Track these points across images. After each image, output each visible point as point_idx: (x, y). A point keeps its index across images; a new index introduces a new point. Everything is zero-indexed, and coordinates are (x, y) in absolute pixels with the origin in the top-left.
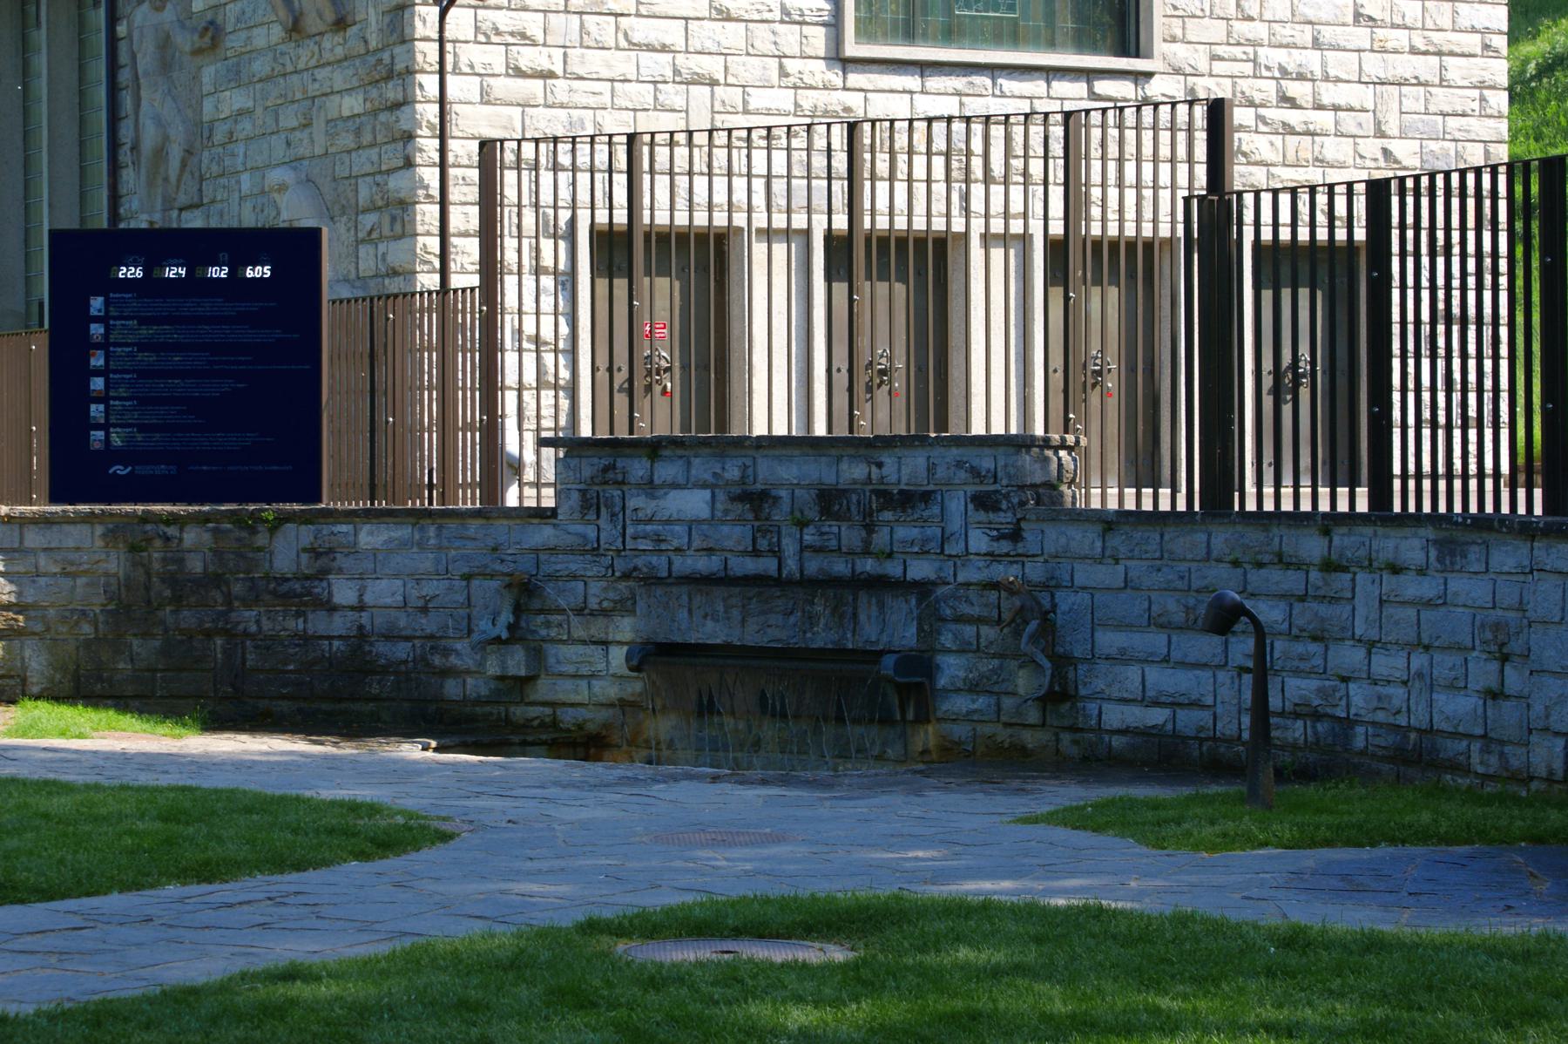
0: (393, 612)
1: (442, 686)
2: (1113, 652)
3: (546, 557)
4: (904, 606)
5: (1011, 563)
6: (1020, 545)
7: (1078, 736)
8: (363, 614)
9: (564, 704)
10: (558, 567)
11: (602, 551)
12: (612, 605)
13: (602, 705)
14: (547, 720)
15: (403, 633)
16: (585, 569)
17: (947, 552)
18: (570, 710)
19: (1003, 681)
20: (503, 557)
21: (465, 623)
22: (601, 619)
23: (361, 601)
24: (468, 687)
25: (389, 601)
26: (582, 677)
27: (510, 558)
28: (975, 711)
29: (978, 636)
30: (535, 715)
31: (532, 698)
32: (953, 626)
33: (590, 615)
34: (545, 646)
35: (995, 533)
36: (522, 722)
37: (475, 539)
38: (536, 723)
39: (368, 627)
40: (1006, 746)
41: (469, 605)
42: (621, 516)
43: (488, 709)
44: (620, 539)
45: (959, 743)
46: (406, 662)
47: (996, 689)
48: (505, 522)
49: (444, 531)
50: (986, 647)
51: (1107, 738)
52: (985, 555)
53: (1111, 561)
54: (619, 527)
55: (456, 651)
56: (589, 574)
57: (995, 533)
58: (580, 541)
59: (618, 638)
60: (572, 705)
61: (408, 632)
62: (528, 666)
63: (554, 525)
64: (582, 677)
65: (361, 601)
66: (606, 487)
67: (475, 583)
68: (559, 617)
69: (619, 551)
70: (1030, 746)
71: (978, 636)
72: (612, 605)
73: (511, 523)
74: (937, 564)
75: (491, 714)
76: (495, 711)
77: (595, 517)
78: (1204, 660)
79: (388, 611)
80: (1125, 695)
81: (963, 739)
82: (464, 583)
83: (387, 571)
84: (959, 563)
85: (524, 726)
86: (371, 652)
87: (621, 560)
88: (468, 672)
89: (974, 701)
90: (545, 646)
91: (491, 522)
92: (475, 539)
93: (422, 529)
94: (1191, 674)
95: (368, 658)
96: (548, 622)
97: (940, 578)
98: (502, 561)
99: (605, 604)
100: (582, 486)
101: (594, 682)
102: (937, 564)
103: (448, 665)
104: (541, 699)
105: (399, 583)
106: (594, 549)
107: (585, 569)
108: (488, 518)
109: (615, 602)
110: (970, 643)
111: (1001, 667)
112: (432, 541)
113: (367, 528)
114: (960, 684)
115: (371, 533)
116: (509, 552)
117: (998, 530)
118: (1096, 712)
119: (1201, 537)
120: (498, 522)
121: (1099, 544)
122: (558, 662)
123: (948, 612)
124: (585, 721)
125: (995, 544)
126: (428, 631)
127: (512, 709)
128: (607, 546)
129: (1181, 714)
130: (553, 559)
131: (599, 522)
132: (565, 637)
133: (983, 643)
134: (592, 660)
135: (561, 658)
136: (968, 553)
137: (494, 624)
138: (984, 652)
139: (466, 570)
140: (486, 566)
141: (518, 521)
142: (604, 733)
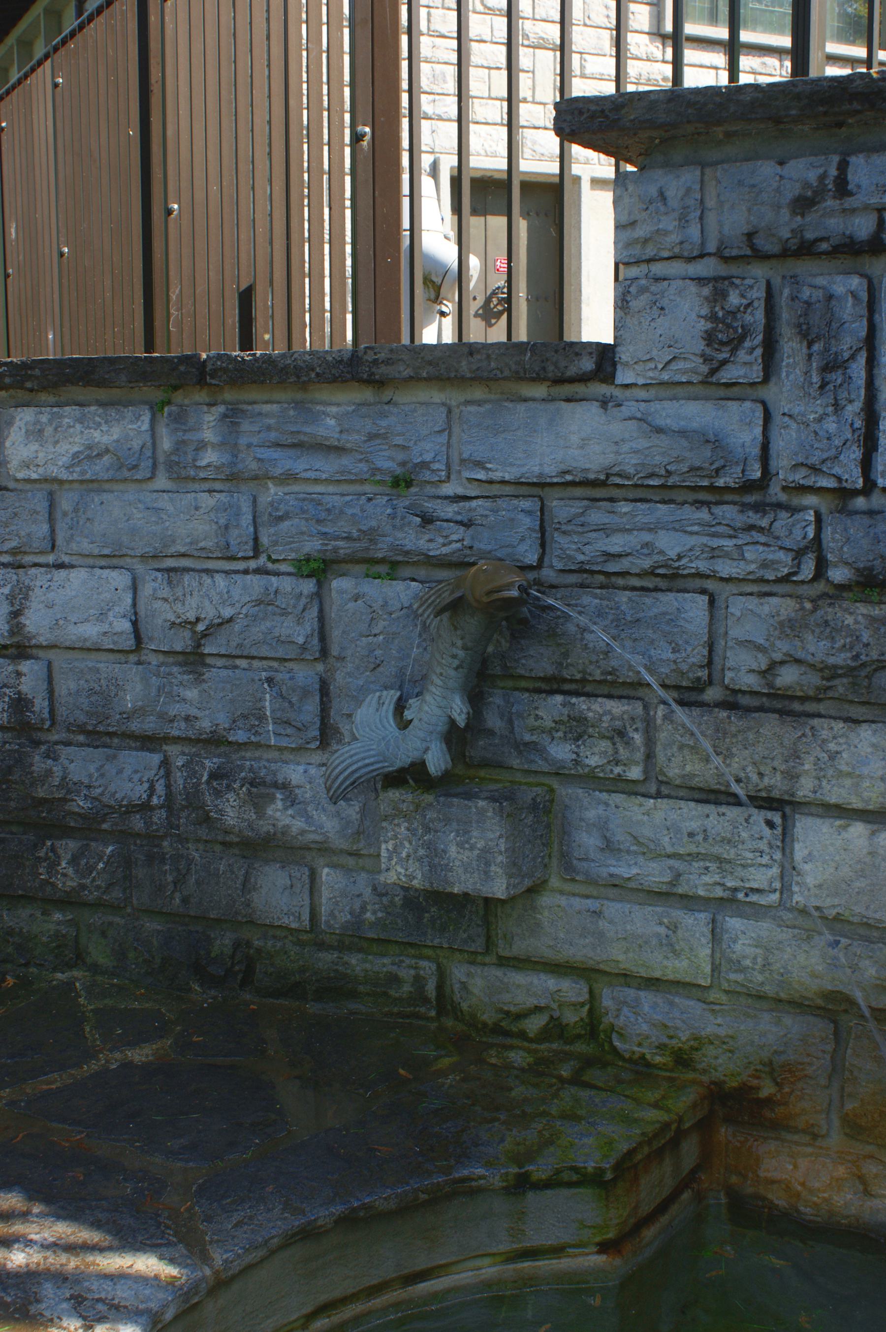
0: (107, 667)
1: (247, 886)
3: (576, 508)
8: (25, 666)
9: (626, 978)
10: (616, 543)
11: (775, 492)
12: (815, 679)
13: (760, 997)
14: (571, 1017)
15: (135, 726)
16: (714, 554)
18: (647, 999)
20: (429, 505)
21: (312, 707)
22: (770, 725)
23: (16, 629)
24: (325, 894)
25: (91, 631)
26: (690, 901)
27: (450, 510)
30: (531, 1002)
31: (519, 948)
33: (730, 705)
34: (566, 792)
36: (488, 1017)
37: (339, 450)
38: (534, 1025)
39: (40, 704)
41: (324, 652)
42: (858, 370)
43: (383, 964)
44: (855, 453)
46: (145, 807)
48: (437, 396)
49: (246, 426)
54: (853, 409)
55: (285, 786)
56: (726, 568)
58: (701, 457)
59: (835, 794)
60: (652, 983)
61: (149, 725)
62: (514, 867)
63: (604, 403)
64: (690, 901)
65: (16, 629)
66: (803, 267)
67: (341, 586)
68: (617, 707)
69: (844, 494)
72: (815, 679)
73: (454, 397)
75: (394, 979)
76: (406, 974)
77: (756, 373)
79: (90, 661)
82: (308, 586)
83: (86, 546)
85: (497, 1030)
86: (49, 773)
87: (856, 528)
88: (324, 849)
90: (566, 792)
91: (387, 395)
92: (339, 450)
93: (179, 419)
95: (41, 793)
96: (581, 720)
98: (427, 520)
99: (788, 677)
100: (707, 267)
101: (734, 924)
103: (265, 827)
104: (549, 954)
105: (119, 579)
106: (748, 487)
107: (714, 554)
108: (379, 383)
109: (830, 673)
112: (210, 457)
113: (25, 417)
115: (36, 433)
116: (448, 489)
120: (407, 398)
122: (610, 847)
124: (699, 1042)
126: (206, 724)
127: (458, 972)
128: (799, 477)
130: (596, 516)
131: (770, 393)
132: (635, 773)
134: (729, 853)
135: (619, 836)
137: (404, 725)
139: (312, 546)
140: (371, 535)
141: (478, 393)
142: (767, 1089)
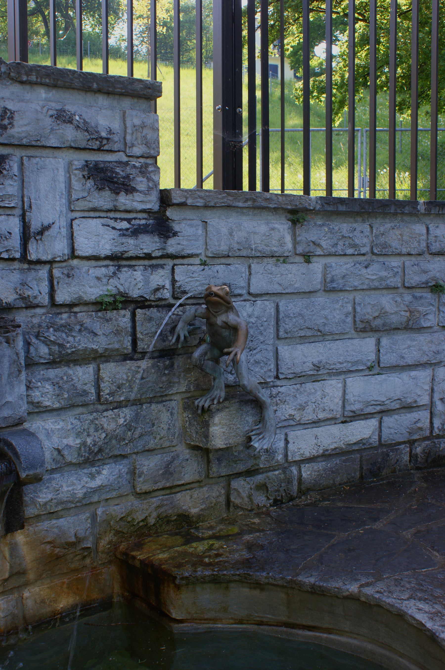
2: (308, 368)
4: (7, 351)
5: (153, 267)
6: (172, 241)
7: (260, 478)
17: (33, 256)
19: (141, 435)
28: (95, 490)
29: (98, 380)
32: (52, 373)
35: (125, 225)
40: (152, 521)
45: (79, 540)
47: (128, 450)
50: (111, 394)
51: (294, 470)
52: (107, 258)
53: (301, 259)
57: (125, 225)
70: (194, 511)
71: (98, 380)
74: (16, 277)
78: (425, 359)
80: (321, 416)
81: (81, 534)
84: (56, 273)
89: (92, 477)
94: (405, 376)
97: (23, 298)
102: (16, 277)
110: (85, 393)
111: (136, 418)
114: (71, 457)
117: (129, 221)
118: (282, 444)
119: (420, 229)
121: (288, 239)
123: (44, 350)
125: (131, 241)
129: (388, 421)
133: (106, 388)
136: (73, 255)
138: (107, 402)
